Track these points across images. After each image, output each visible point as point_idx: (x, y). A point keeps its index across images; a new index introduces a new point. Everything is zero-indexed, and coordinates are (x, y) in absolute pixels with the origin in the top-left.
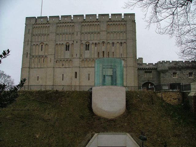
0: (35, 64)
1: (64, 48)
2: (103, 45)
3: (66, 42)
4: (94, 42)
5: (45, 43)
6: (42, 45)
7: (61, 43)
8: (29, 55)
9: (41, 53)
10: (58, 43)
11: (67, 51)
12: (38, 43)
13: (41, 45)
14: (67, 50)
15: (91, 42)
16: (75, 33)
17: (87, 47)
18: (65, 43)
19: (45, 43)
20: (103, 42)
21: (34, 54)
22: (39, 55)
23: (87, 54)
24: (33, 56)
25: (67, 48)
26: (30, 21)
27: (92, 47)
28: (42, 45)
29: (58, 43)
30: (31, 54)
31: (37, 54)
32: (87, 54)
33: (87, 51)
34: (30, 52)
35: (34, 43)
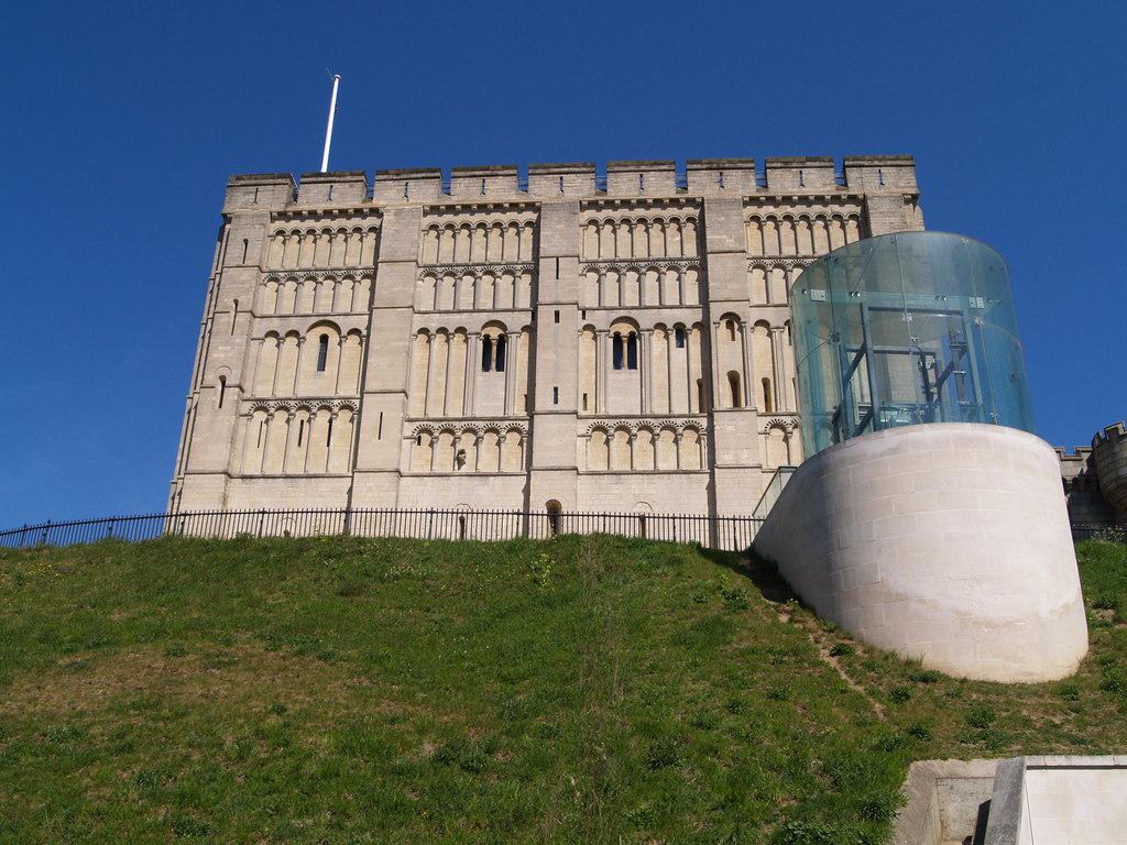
0: (272, 449)
1: (465, 354)
2: (733, 339)
3: (485, 318)
4: (670, 317)
5: (346, 324)
6: (324, 339)
7: (453, 322)
8: (232, 394)
9: (312, 386)
10: (433, 327)
11: (493, 372)
12: (294, 324)
13: (313, 338)
14: (494, 364)
15: (646, 319)
16: (546, 266)
17: (626, 351)
18: (474, 323)
19: (346, 324)
20: (732, 319)
21: (263, 391)
22: (301, 394)
23: (622, 394)
24: (261, 405)
25: (494, 354)
26: (252, 197)
27: (655, 347)
28: (324, 339)
29: (433, 327)
30: (246, 386)
31: (284, 391)
32: (622, 394)
33: (627, 377)
34: (242, 376)
35: (275, 325)
